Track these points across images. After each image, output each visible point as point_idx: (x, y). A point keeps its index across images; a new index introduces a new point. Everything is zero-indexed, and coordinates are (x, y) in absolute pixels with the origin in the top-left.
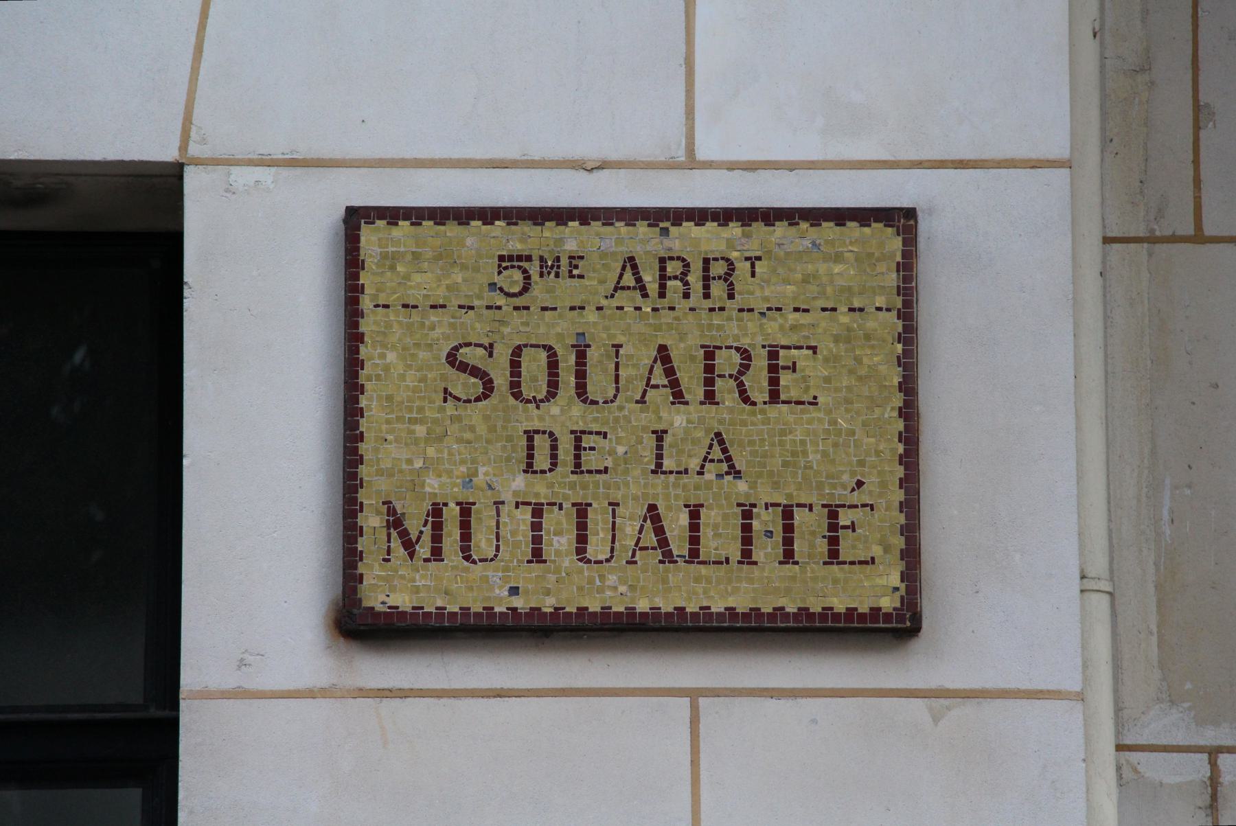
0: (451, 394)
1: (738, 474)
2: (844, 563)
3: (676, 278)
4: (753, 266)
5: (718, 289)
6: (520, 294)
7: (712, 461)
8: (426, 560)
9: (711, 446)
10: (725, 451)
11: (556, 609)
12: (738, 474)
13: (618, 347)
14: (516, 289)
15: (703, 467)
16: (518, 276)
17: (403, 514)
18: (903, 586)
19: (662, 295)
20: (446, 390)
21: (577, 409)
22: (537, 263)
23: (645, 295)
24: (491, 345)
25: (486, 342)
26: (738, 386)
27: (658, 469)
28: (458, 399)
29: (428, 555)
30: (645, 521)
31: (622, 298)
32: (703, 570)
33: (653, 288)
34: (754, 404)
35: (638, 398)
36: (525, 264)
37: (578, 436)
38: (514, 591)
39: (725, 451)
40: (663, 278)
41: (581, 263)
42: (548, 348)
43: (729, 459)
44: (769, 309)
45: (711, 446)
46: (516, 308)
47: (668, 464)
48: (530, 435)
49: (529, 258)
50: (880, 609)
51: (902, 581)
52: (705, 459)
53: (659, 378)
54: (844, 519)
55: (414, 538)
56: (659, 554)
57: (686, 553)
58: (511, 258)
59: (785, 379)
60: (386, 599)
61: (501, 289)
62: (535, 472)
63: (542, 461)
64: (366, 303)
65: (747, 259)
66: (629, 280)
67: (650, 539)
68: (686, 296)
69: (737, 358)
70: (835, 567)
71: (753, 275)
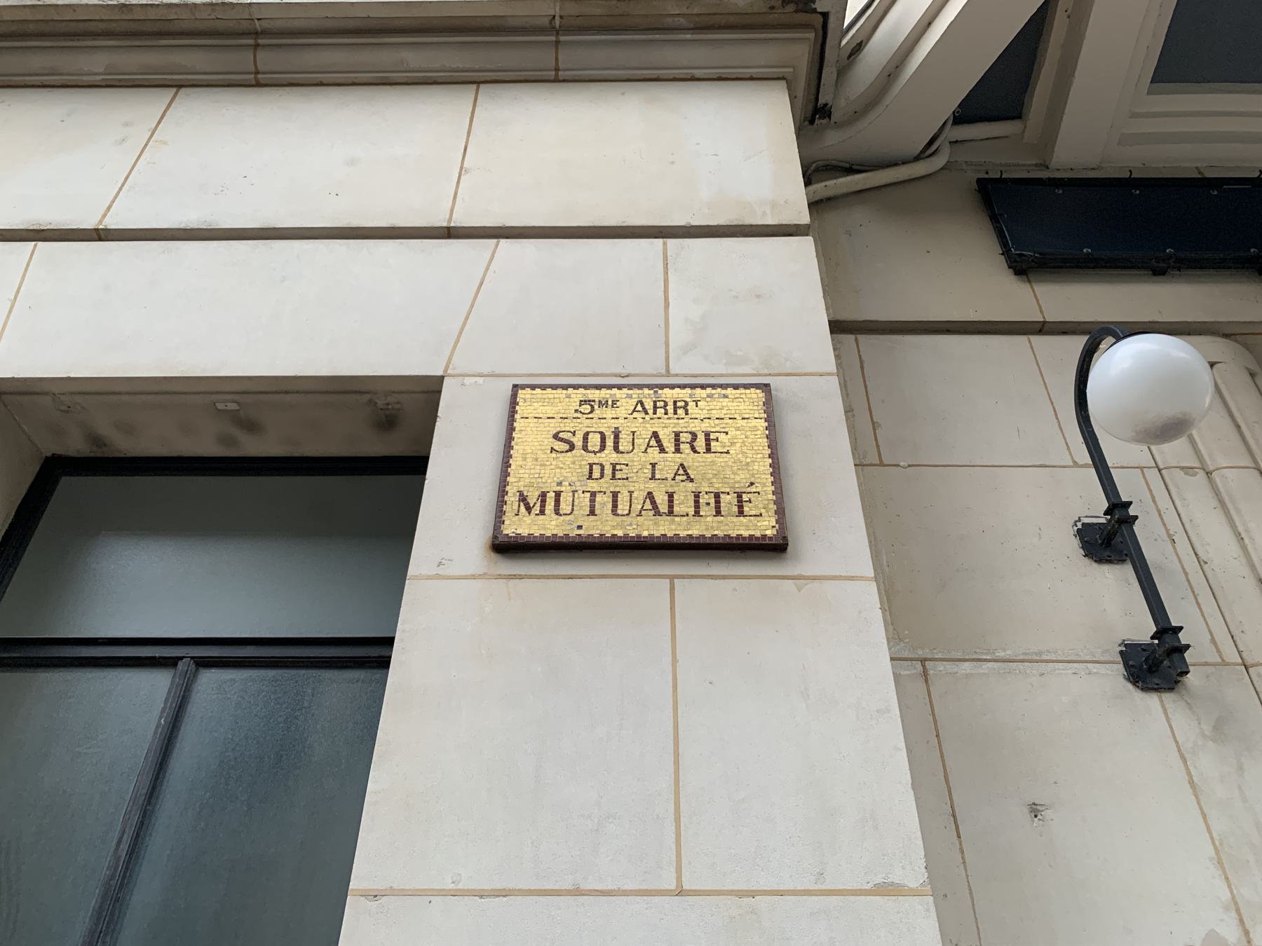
0: (554, 450)
1: (692, 480)
2: (746, 516)
3: (661, 407)
4: (697, 404)
5: (681, 412)
6: (589, 413)
7: (679, 475)
8: (536, 515)
9: (678, 469)
10: (685, 471)
11: (601, 535)
12: (692, 480)
13: (634, 433)
14: (587, 412)
15: (675, 477)
16: (588, 407)
17: (527, 496)
18: (777, 526)
19: (655, 413)
20: (552, 448)
21: (615, 455)
22: (597, 403)
23: (647, 413)
24: (575, 432)
25: (572, 430)
26: (691, 446)
27: (653, 478)
28: (558, 451)
29: (538, 512)
30: (646, 498)
31: (635, 414)
32: (677, 519)
33: (651, 412)
34: (699, 453)
35: (643, 450)
36: (593, 403)
37: (614, 466)
38: (580, 527)
39: (685, 471)
40: (655, 407)
41: (618, 403)
42: (601, 433)
43: (687, 474)
44: (705, 418)
45: (678, 469)
46: (587, 418)
47: (657, 476)
48: (591, 465)
49: (594, 401)
50: (766, 535)
51: (777, 523)
52: (676, 474)
53: (653, 443)
54: (745, 497)
55: (531, 505)
56: (653, 512)
57: (667, 511)
58: (585, 401)
59: (713, 444)
60: (515, 531)
61: (581, 412)
62: (593, 479)
63: (596, 474)
64: (517, 416)
65: (694, 401)
66: (639, 408)
67: (648, 505)
68: (666, 414)
69: (690, 436)
70: (742, 518)
71: (697, 406)
